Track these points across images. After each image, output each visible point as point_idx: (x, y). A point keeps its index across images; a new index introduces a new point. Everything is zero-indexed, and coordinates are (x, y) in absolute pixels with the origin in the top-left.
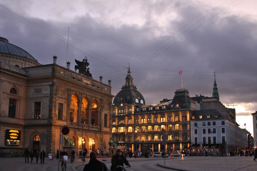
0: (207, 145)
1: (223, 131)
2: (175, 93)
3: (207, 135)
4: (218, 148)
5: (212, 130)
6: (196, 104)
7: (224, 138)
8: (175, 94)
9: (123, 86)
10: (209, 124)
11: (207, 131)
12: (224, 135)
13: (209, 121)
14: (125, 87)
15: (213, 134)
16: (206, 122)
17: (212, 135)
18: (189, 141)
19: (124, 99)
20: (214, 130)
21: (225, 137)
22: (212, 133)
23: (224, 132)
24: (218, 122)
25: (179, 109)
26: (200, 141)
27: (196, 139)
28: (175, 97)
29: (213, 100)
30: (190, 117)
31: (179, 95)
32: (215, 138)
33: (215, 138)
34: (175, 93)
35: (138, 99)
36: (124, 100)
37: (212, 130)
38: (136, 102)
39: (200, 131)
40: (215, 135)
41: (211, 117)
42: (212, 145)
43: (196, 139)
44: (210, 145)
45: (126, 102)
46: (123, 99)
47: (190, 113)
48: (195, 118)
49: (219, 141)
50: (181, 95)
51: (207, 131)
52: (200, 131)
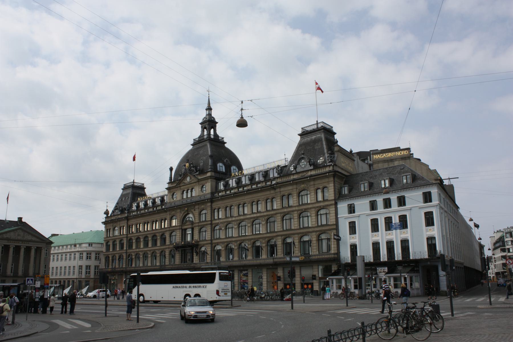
0: (384, 264)
1: (429, 220)
2: (299, 135)
3: (382, 237)
4: (418, 271)
5: (396, 220)
6: (354, 160)
7: (433, 242)
8: (299, 138)
9: (194, 140)
10: (387, 204)
11: (382, 224)
12: (435, 231)
13: (386, 196)
14: (198, 141)
15: (398, 231)
16: (380, 200)
17: (396, 236)
18: (334, 254)
19: (192, 165)
20: (403, 220)
21: (435, 238)
22: (396, 229)
23: (433, 224)
24: (413, 198)
25: (308, 171)
26: (366, 253)
27: (354, 248)
28: (300, 146)
29: (399, 154)
30: (337, 190)
31: (308, 139)
32: (405, 244)
33: (405, 244)
34: (299, 135)
35: (224, 165)
36: (193, 167)
37: (396, 220)
38: (218, 170)
39: (364, 225)
40: (406, 234)
41: (392, 182)
42: (399, 263)
43: (354, 248)
44: (392, 265)
45: (197, 172)
46: (190, 165)
47: (336, 179)
48: (350, 191)
49: (419, 251)
50: (314, 137)
51: (382, 224)
52: (364, 225)
